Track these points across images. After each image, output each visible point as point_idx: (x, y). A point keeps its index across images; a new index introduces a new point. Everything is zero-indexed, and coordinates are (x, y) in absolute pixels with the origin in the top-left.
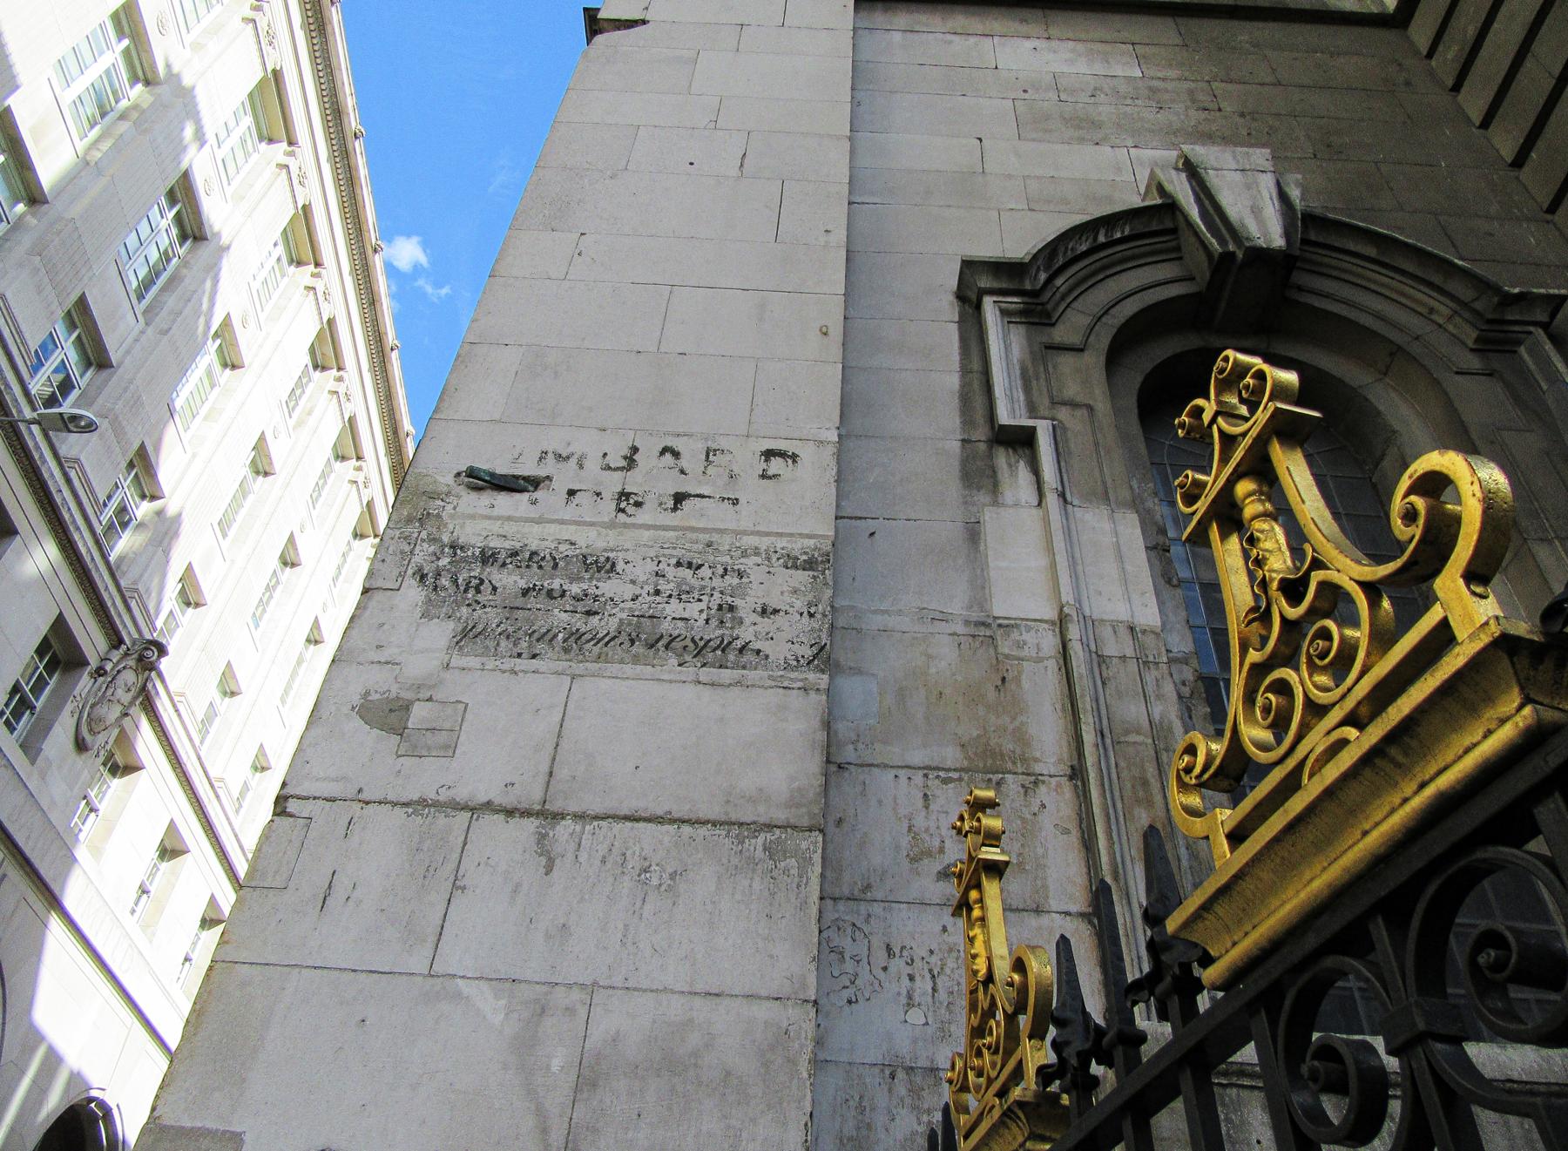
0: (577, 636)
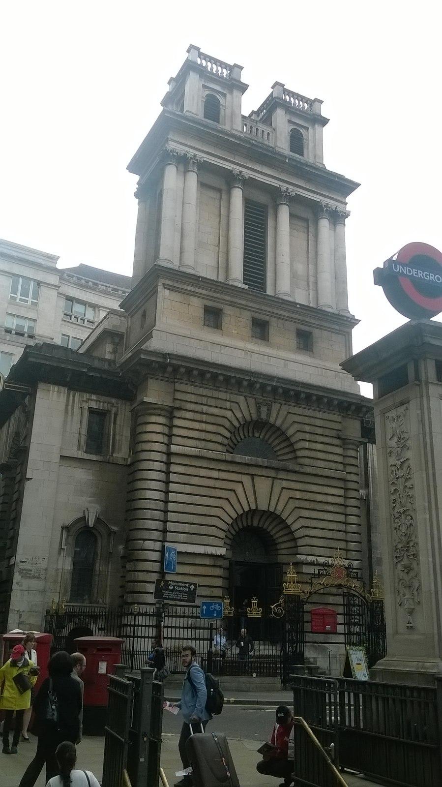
0: (29, 577)
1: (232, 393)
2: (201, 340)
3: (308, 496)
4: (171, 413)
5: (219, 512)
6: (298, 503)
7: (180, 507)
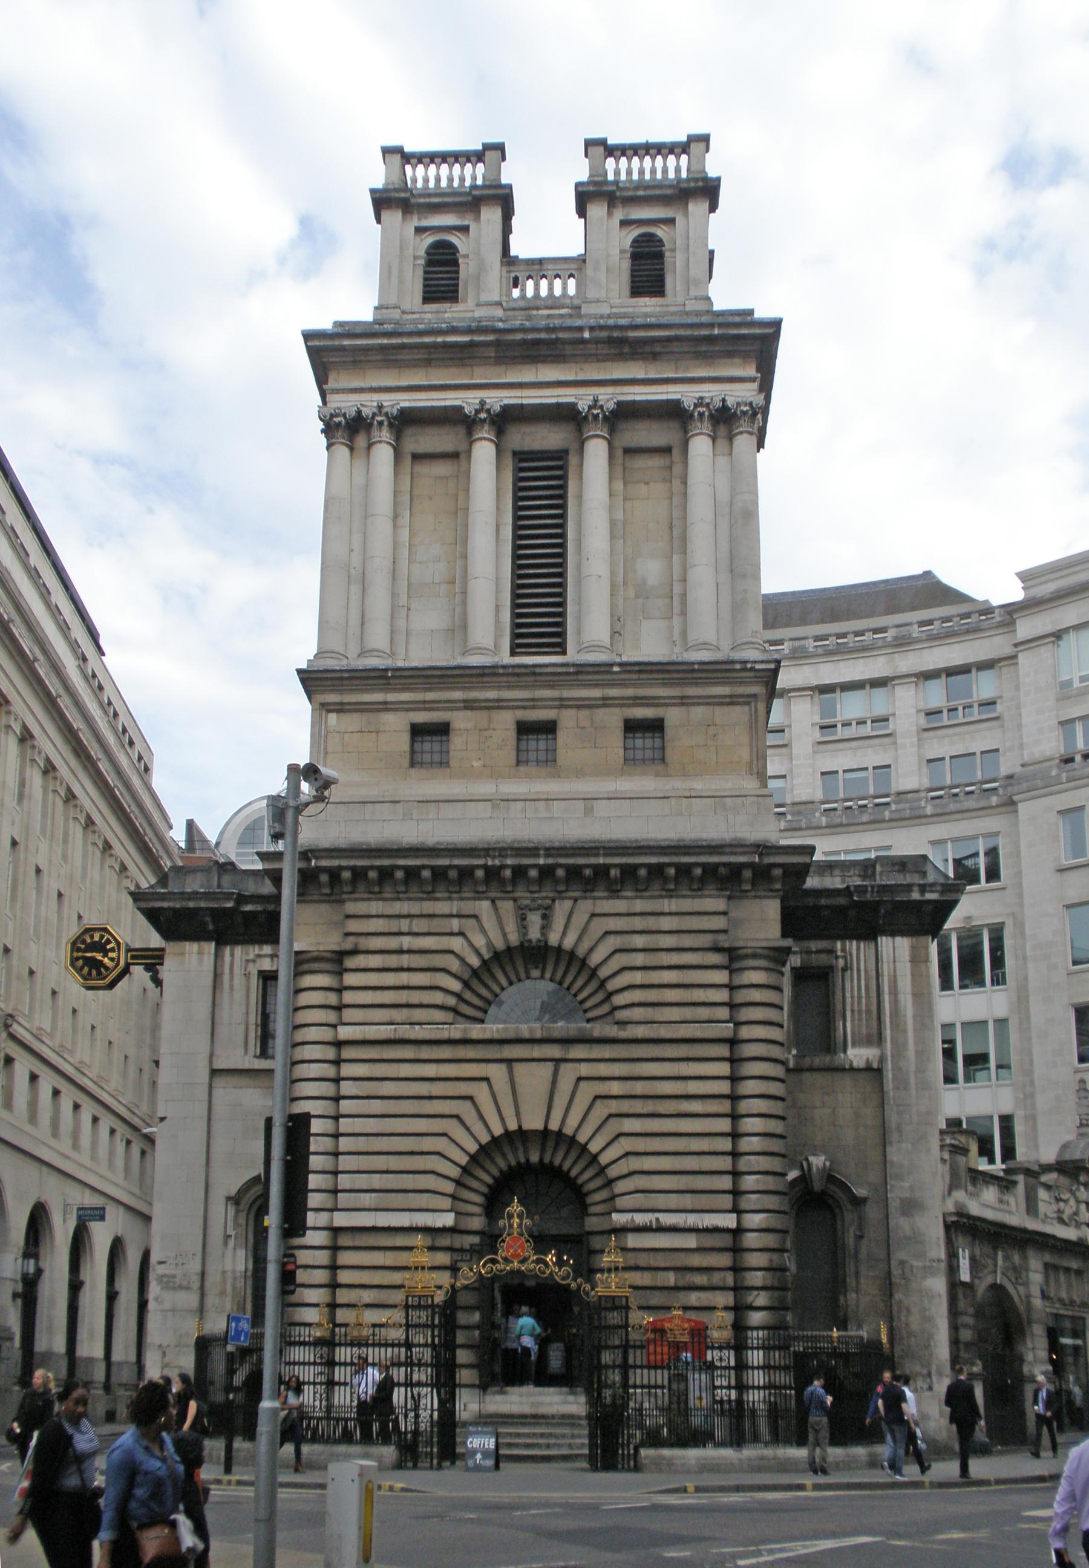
1: (462, 899)
2: (398, 802)
3: (639, 1088)
4: (340, 962)
5: (440, 1144)
6: (614, 1106)
7: (362, 1144)
